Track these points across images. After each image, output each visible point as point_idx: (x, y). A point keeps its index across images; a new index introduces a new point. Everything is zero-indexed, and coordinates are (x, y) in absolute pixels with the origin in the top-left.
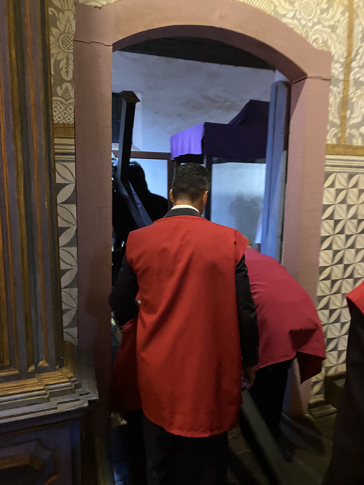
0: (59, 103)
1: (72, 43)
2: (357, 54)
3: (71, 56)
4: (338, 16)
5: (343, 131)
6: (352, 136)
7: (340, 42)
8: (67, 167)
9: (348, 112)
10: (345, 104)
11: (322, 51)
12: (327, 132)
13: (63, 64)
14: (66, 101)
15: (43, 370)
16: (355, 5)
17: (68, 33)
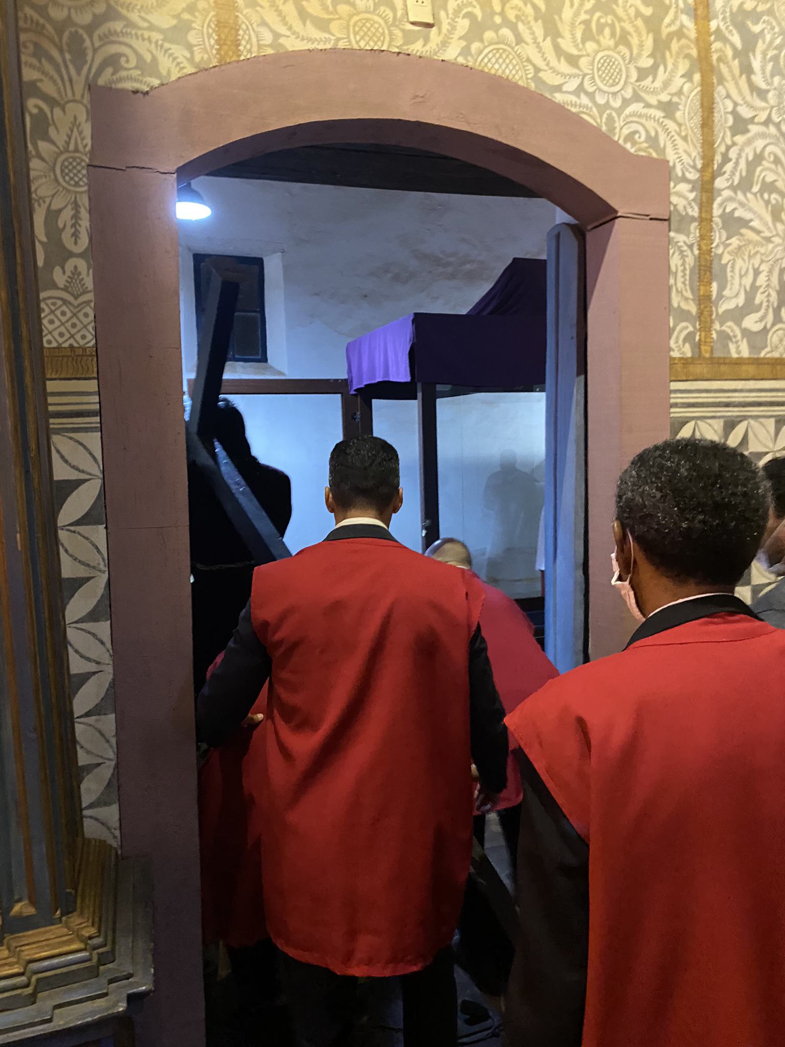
0: (59, 302)
1: (84, 172)
2: (726, 159)
3: (84, 201)
4: (678, 81)
5: (706, 327)
6: (725, 338)
7: (685, 139)
8: (81, 444)
9: (715, 286)
10: (706, 269)
11: (650, 159)
12: (670, 332)
13: (66, 216)
14: (76, 298)
15: (26, 924)
16: (715, 57)
17: (76, 150)
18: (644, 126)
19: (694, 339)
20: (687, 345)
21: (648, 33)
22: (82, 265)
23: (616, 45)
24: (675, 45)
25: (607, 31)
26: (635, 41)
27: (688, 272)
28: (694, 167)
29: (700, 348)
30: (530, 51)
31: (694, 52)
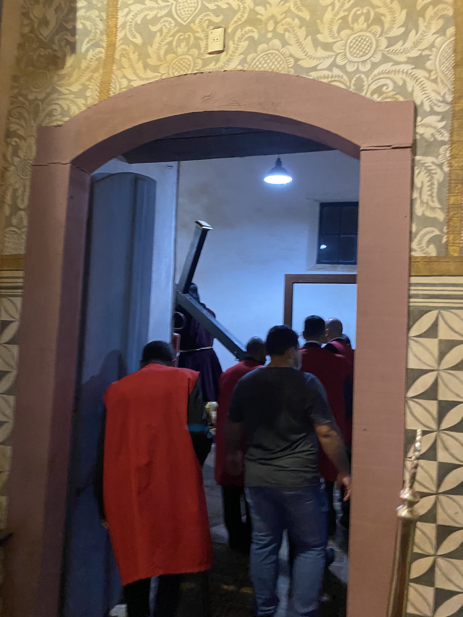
3: (28, 183)
7: (435, 81)
11: (396, 104)
18: (392, 80)
19: (441, 241)
20: (432, 246)
21: (402, 9)
22: (23, 213)
23: (369, 26)
24: (430, 12)
25: (362, 18)
26: (387, 20)
27: (436, 186)
28: (444, 101)
29: (447, 249)
30: (294, 49)
31: (450, 12)
